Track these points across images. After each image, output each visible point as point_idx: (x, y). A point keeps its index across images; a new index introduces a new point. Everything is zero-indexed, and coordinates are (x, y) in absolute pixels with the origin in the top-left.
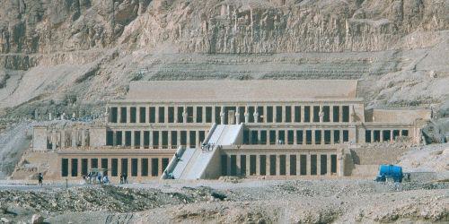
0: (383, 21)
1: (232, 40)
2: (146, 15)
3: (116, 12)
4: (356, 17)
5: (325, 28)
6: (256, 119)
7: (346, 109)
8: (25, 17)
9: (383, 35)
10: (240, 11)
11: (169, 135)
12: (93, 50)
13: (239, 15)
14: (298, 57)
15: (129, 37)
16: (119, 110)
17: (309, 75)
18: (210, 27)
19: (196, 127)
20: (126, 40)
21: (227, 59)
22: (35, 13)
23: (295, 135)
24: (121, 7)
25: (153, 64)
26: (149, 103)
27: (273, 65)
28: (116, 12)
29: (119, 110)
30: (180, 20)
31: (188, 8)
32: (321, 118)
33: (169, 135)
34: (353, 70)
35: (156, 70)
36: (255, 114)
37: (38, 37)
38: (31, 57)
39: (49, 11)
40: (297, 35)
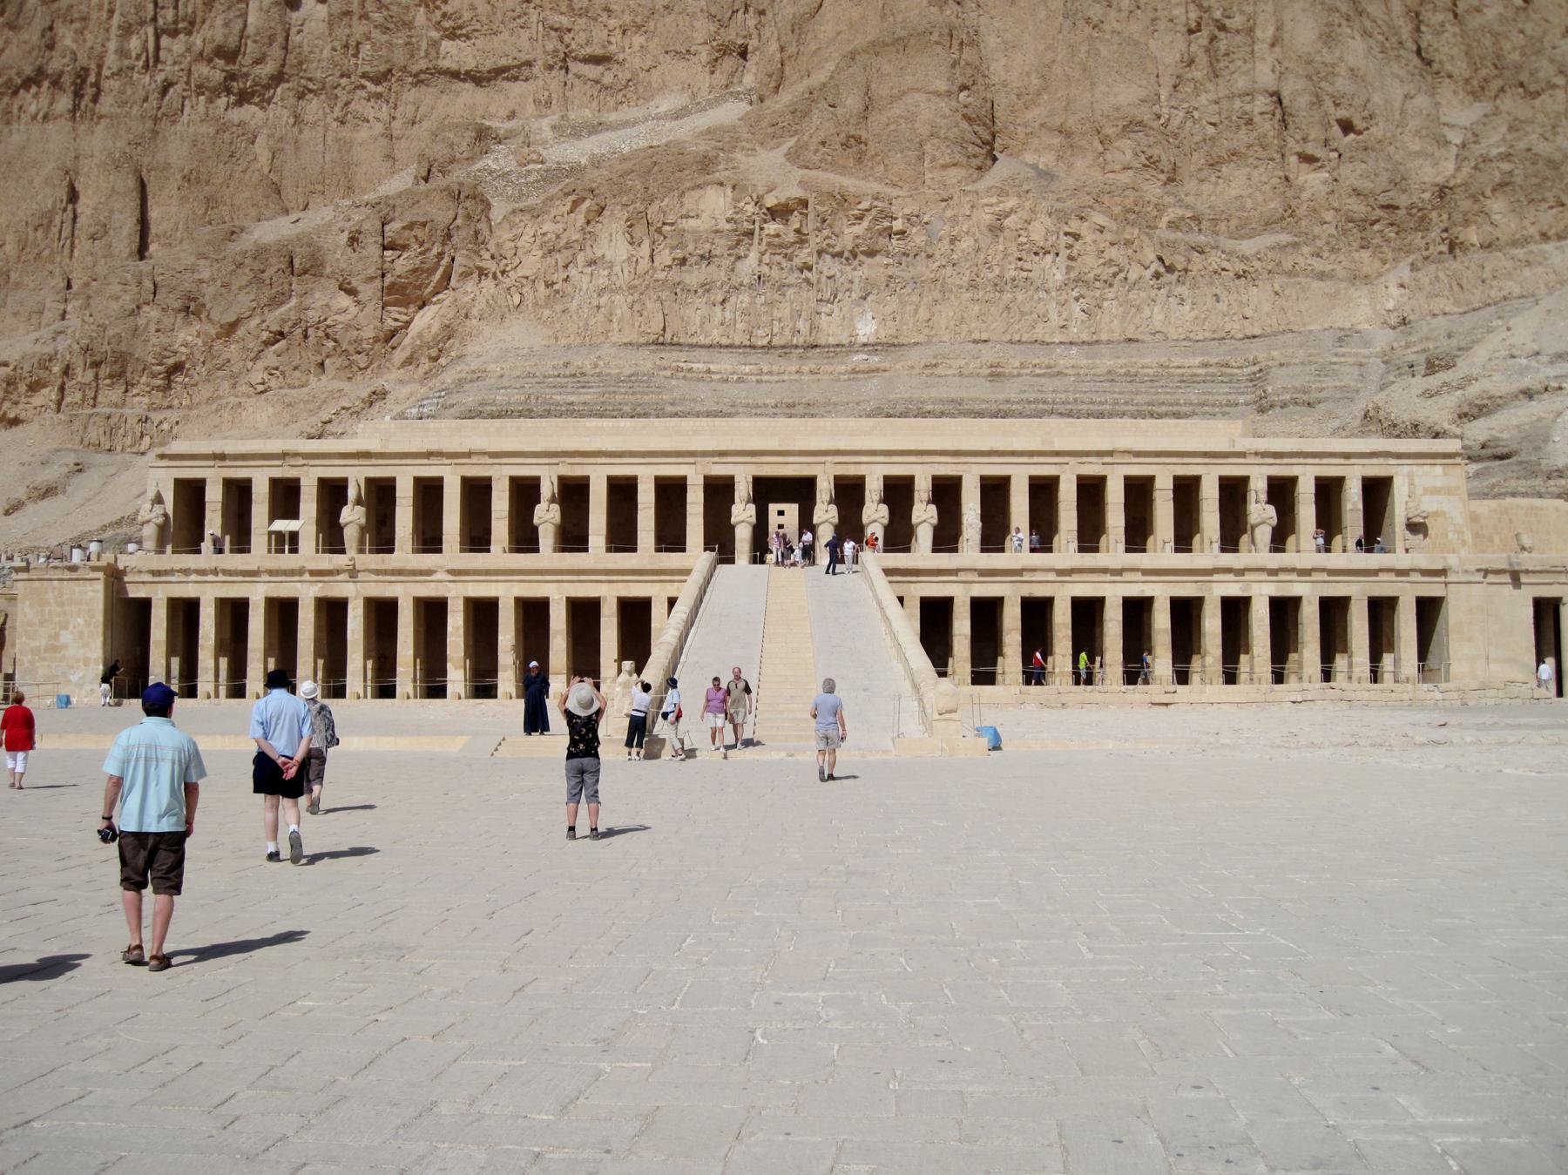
0: (1284, 238)
1: (744, 298)
3: (388, 280)
6: (924, 536)
7: (1377, 491)
8: (151, 313)
9: (1278, 282)
10: (770, 201)
11: (456, 622)
12: (320, 385)
14: (988, 354)
16: (214, 496)
17: (1040, 411)
18: (664, 257)
19: (602, 575)
20: (409, 361)
21: (725, 364)
22: (177, 305)
23: (1161, 620)
24: (402, 264)
25: (460, 383)
27: (904, 381)
28: (388, 280)
29: (214, 496)
30: (563, 242)
31: (587, 203)
32: (1264, 534)
33: (456, 622)
36: (924, 514)
37: (178, 368)
38: (156, 417)
39: (208, 290)
40: (973, 286)
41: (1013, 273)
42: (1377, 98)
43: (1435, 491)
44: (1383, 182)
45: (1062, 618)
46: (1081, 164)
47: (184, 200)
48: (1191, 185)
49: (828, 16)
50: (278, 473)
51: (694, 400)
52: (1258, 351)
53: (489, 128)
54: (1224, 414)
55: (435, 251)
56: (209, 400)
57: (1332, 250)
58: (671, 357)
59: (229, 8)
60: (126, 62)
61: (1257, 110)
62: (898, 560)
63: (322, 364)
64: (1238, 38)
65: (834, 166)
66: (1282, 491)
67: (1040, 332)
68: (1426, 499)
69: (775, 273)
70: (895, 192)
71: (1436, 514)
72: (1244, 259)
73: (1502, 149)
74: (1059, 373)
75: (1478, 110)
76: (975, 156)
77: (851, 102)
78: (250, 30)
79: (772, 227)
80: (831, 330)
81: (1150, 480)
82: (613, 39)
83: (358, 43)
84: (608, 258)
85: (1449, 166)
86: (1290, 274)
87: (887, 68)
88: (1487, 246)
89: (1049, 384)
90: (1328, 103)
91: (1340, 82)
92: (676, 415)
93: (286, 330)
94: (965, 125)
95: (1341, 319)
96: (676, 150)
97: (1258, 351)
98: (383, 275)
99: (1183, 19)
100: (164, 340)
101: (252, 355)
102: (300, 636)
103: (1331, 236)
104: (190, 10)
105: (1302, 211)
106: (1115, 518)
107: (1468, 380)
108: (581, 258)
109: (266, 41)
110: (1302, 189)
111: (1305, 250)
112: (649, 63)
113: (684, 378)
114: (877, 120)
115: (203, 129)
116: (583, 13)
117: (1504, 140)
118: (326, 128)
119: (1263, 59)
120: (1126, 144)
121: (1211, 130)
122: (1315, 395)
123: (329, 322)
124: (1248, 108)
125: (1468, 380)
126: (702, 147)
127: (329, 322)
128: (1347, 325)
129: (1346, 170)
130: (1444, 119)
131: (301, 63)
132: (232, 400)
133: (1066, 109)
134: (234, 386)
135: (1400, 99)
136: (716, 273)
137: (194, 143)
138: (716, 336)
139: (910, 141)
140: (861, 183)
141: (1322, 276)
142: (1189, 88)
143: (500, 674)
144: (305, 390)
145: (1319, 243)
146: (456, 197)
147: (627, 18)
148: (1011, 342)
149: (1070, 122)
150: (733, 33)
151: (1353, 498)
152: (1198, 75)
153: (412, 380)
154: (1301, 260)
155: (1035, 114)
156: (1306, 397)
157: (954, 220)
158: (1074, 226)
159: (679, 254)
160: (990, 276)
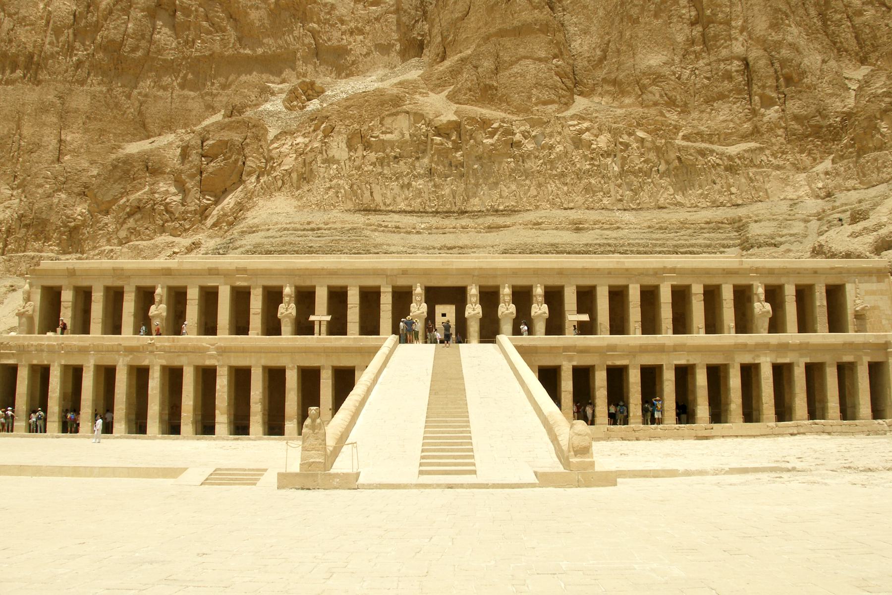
1: (421, 181)
2: (253, 179)
4: (685, 138)
5: (624, 159)
6: (540, 326)
7: (835, 294)
9: (752, 171)
11: (222, 384)
13: (438, 132)
14: (573, 215)
15: (225, 215)
20: (214, 225)
23: (701, 379)
26: (167, 272)
30: (309, 149)
31: (324, 125)
33: (222, 384)
34: (701, 241)
35: (250, 240)
36: (540, 310)
40: (563, 175)
41: (588, 167)
42: (806, 61)
43: (873, 293)
44: (813, 108)
45: (634, 378)
46: (627, 101)
47: (86, 131)
48: (695, 114)
49: (473, 19)
50: (110, 283)
51: (388, 245)
52: (741, 212)
53: (269, 87)
54: (721, 253)
55: (233, 158)
56: (95, 248)
57: (783, 153)
58: (374, 219)
59: (118, 18)
60: (56, 49)
61: (734, 69)
62: (525, 339)
63: (163, 226)
64: (721, 26)
65: (476, 102)
66: (774, 295)
67: (605, 201)
68: (867, 298)
69: (440, 168)
70: (515, 118)
71: (874, 308)
72: (730, 158)
73: (885, 90)
74: (618, 228)
75: (865, 70)
76: (563, 97)
77: (487, 64)
78: (130, 31)
79: (438, 139)
80: (475, 204)
81: (689, 287)
82: (344, 37)
83: (194, 42)
84: (337, 157)
85: (851, 102)
86: (759, 166)
87: (509, 45)
88: (880, 149)
89: (614, 234)
90: (777, 65)
91: (783, 51)
92: (378, 253)
93: (142, 205)
94: (558, 78)
95: (790, 193)
96: (379, 92)
97: (741, 212)
98: (201, 172)
99: (687, 16)
100: (69, 212)
101: (121, 220)
102: (117, 391)
103: (782, 144)
104: (95, 19)
105: (764, 129)
106: (666, 313)
107: (880, 226)
108: (319, 158)
109: (139, 37)
110: (763, 115)
111: (767, 152)
112: (365, 51)
113: (383, 231)
114: (504, 75)
115: (98, 89)
116: (327, 22)
117: (885, 85)
118: (173, 89)
119: (737, 39)
120: (654, 89)
121: (706, 82)
122: (779, 239)
123: (167, 200)
124: (729, 67)
125: (880, 226)
126: (395, 91)
127: (167, 200)
128: (795, 197)
129: (789, 104)
130: (845, 75)
131: (159, 51)
132: (108, 248)
133: (617, 69)
134: (109, 241)
135: (819, 62)
136: (402, 167)
137: (94, 97)
138: (402, 206)
139: (524, 87)
140: (494, 113)
141: (778, 168)
142: (692, 57)
143: (252, 418)
144: (152, 241)
145: (775, 148)
146: (246, 124)
147: (352, 25)
148: (587, 209)
149: (621, 77)
150: (415, 32)
151: (820, 300)
152: (697, 48)
153: (217, 236)
154: (764, 158)
155: (601, 74)
156: (773, 241)
157: (551, 136)
158: (625, 138)
159: (381, 154)
160: (574, 169)
